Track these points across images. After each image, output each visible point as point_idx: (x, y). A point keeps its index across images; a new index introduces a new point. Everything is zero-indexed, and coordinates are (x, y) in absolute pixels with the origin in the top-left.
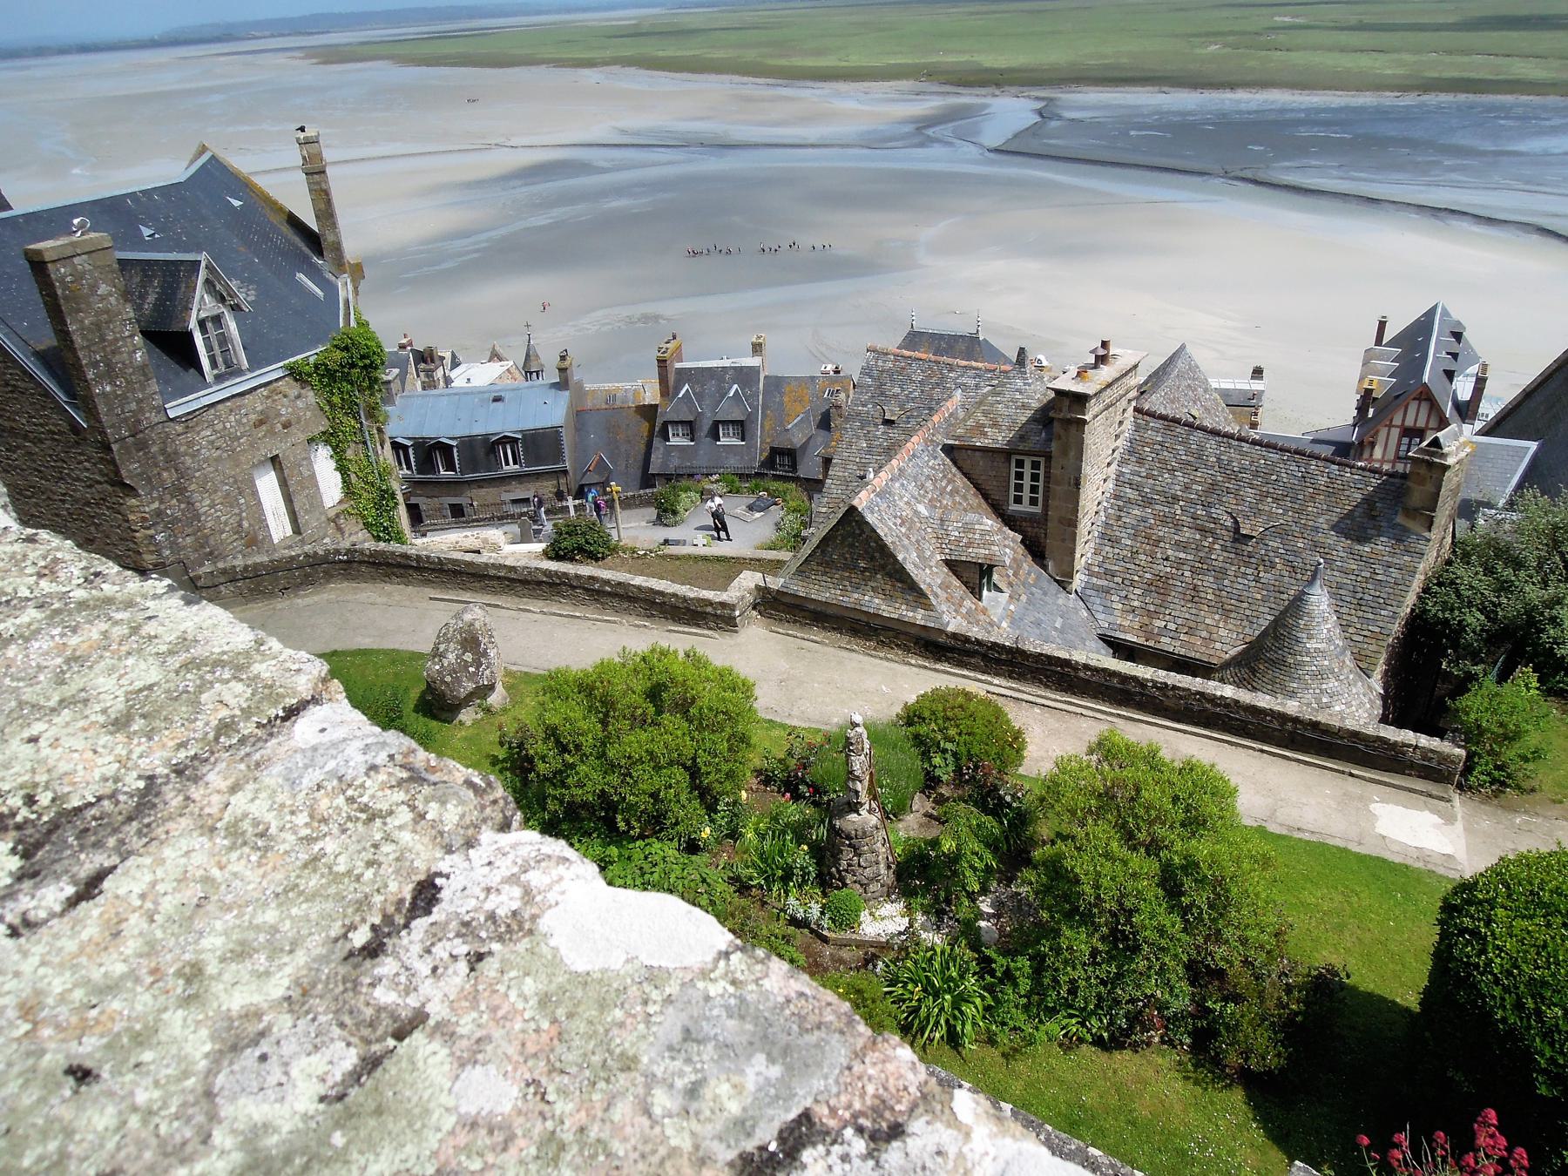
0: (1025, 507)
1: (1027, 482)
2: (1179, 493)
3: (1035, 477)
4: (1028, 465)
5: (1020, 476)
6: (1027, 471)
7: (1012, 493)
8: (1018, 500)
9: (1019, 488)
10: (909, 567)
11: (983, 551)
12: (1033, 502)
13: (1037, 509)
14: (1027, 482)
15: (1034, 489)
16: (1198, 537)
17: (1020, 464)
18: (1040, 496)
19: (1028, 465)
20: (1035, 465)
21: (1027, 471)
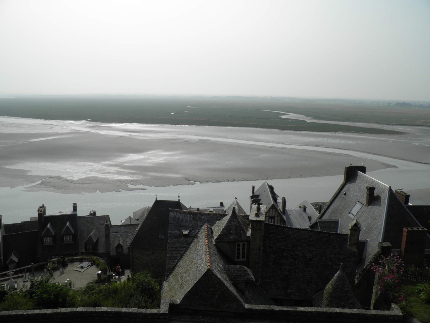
0: (241, 259)
1: (241, 251)
2: (285, 248)
3: (244, 249)
4: (241, 244)
5: (239, 249)
6: (241, 247)
7: (236, 255)
8: (238, 257)
9: (238, 253)
10: (229, 287)
11: (246, 278)
12: (243, 257)
13: (245, 260)
14: (241, 251)
15: (243, 253)
16: (293, 261)
17: (239, 245)
18: (245, 255)
19: (241, 244)
20: (244, 245)
21: (241, 247)
